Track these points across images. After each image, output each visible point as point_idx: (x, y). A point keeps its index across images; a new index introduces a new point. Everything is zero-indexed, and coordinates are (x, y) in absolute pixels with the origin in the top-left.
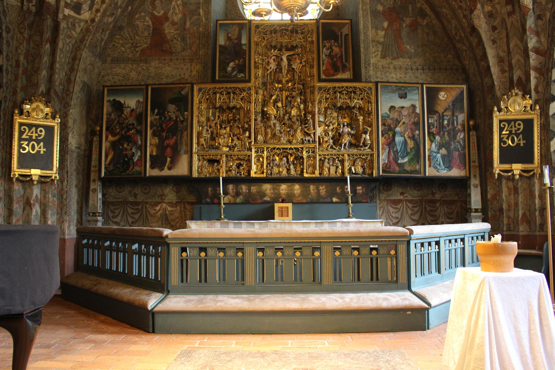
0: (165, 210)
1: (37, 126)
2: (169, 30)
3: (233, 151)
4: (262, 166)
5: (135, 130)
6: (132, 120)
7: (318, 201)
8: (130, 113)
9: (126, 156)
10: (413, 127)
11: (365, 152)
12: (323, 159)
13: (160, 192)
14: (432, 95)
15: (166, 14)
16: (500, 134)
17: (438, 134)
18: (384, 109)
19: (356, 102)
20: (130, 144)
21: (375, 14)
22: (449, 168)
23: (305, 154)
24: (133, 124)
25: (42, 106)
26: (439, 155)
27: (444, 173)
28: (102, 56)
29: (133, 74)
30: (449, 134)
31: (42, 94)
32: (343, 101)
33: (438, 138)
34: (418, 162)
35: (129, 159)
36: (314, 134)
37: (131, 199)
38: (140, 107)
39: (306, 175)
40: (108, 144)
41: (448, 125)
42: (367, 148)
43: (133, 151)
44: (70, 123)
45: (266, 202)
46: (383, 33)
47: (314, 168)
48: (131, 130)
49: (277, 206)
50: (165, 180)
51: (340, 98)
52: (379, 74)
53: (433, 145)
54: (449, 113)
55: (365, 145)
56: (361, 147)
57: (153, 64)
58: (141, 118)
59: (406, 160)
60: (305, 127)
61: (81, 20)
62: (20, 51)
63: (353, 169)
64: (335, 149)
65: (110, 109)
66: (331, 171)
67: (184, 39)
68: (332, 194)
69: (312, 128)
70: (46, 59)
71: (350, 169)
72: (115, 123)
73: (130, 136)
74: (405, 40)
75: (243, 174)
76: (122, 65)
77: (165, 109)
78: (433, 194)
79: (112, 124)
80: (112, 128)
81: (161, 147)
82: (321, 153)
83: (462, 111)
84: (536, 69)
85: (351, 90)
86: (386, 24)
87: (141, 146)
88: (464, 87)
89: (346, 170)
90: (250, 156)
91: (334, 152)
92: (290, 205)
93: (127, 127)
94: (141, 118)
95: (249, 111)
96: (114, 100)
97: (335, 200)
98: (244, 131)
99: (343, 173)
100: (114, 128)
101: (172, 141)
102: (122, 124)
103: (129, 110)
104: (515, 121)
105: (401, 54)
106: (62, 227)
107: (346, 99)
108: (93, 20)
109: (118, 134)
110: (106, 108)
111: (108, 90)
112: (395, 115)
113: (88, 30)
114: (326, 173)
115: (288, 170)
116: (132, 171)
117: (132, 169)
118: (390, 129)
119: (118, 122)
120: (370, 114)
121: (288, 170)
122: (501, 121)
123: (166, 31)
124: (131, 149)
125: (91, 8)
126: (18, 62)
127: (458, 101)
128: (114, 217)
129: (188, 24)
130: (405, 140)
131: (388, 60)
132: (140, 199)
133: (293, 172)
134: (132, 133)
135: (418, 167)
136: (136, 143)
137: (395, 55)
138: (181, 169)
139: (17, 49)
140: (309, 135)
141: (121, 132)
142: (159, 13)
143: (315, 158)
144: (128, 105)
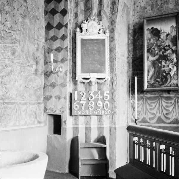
5: (171, 50)
6: (168, 43)
8: (166, 37)
9: (164, 71)
20: (167, 62)
24: (169, 46)
35: (167, 74)
38: (174, 32)
43: (170, 67)
48: (168, 50)
65: (150, 36)
72: (154, 45)
73: (167, 56)
79: (151, 47)
80: (152, 50)
93: (164, 48)
96: (153, 28)
100: (153, 50)
102: (160, 46)
106: (113, 118)
109: (157, 54)
111: (147, 21)
116: (170, 83)
117: (170, 82)
119: (157, 45)
124: (168, 66)
134: (169, 53)
136: (172, 61)
141: (159, 53)
144: (164, 31)
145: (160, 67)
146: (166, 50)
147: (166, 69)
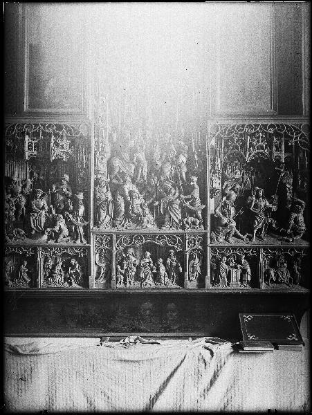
3: (56, 242)
11: (294, 244)
12: (218, 256)
32: (256, 151)
36: (204, 211)
42: (298, 238)
51: (251, 145)
55: (296, 232)
56: (290, 235)
60: (187, 200)
63: (272, 272)
64: (239, 238)
69: (198, 201)
82: (216, 244)
85: (271, 131)
107: (263, 149)
115: (156, 277)
121: (156, 277)
140: (192, 213)
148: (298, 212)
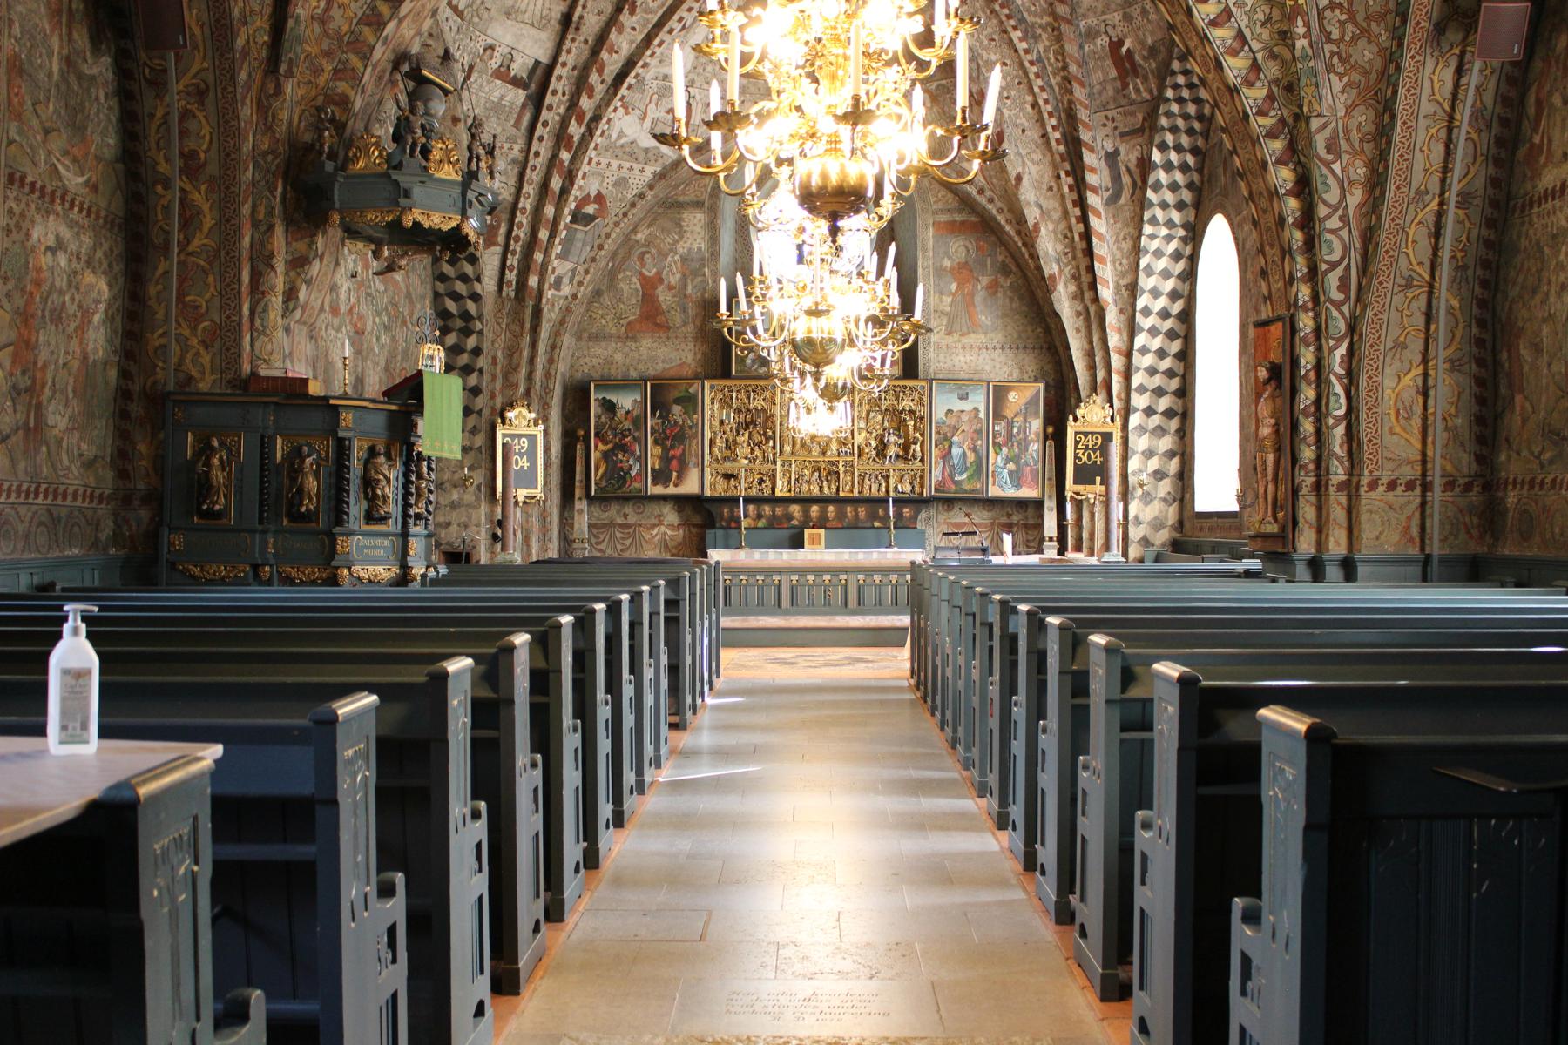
0: (664, 534)
1: (520, 436)
2: (664, 297)
4: (789, 482)
6: (627, 425)
7: (855, 526)
10: (975, 436)
13: (657, 512)
14: (1000, 393)
15: (659, 273)
16: (1076, 449)
17: (1006, 444)
18: (939, 414)
19: (906, 404)
21: (939, 272)
22: (1018, 486)
23: (841, 469)
25: (524, 411)
26: (1005, 471)
27: (1011, 492)
28: (579, 339)
29: (619, 357)
30: (1019, 444)
31: (522, 398)
33: (1005, 450)
34: (979, 478)
35: (626, 474)
37: (620, 520)
39: (842, 494)
40: (599, 455)
41: (1018, 433)
44: (551, 430)
45: (794, 527)
46: (949, 299)
47: (853, 486)
49: (807, 532)
50: (664, 498)
52: (942, 357)
53: (999, 458)
54: (1020, 419)
57: (644, 343)
58: (639, 422)
59: (964, 476)
61: (560, 297)
62: (497, 345)
65: (599, 410)
66: (873, 490)
67: (684, 310)
68: (873, 516)
70: (526, 354)
71: (896, 487)
74: (979, 307)
75: (768, 492)
76: (603, 344)
77: (669, 411)
78: (1009, 516)
81: (666, 459)
83: (1036, 414)
84: (1118, 373)
86: (954, 286)
87: (640, 457)
88: (1041, 386)
89: (891, 489)
90: (775, 470)
91: (877, 466)
92: (822, 532)
94: (639, 422)
95: (773, 416)
97: (876, 524)
98: (767, 440)
99: (887, 491)
101: (678, 452)
102: (615, 429)
103: (623, 411)
104: (1093, 433)
105: (974, 327)
108: (575, 297)
110: (594, 409)
112: (952, 421)
113: (568, 310)
114: (866, 494)
118: (946, 438)
120: (922, 418)
122: (1076, 433)
123: (661, 298)
125: (571, 280)
126: (494, 360)
127: (1033, 401)
128: (597, 543)
129: (690, 288)
130: (964, 452)
131: (955, 337)
132: (631, 520)
133: (826, 490)
135: (978, 486)
136: (633, 453)
137: (965, 329)
138: (690, 486)
139: (493, 342)
142: (650, 272)
143: (853, 473)
145: (616, 462)
146: (625, 436)
147: (625, 465)
148: (915, 443)
